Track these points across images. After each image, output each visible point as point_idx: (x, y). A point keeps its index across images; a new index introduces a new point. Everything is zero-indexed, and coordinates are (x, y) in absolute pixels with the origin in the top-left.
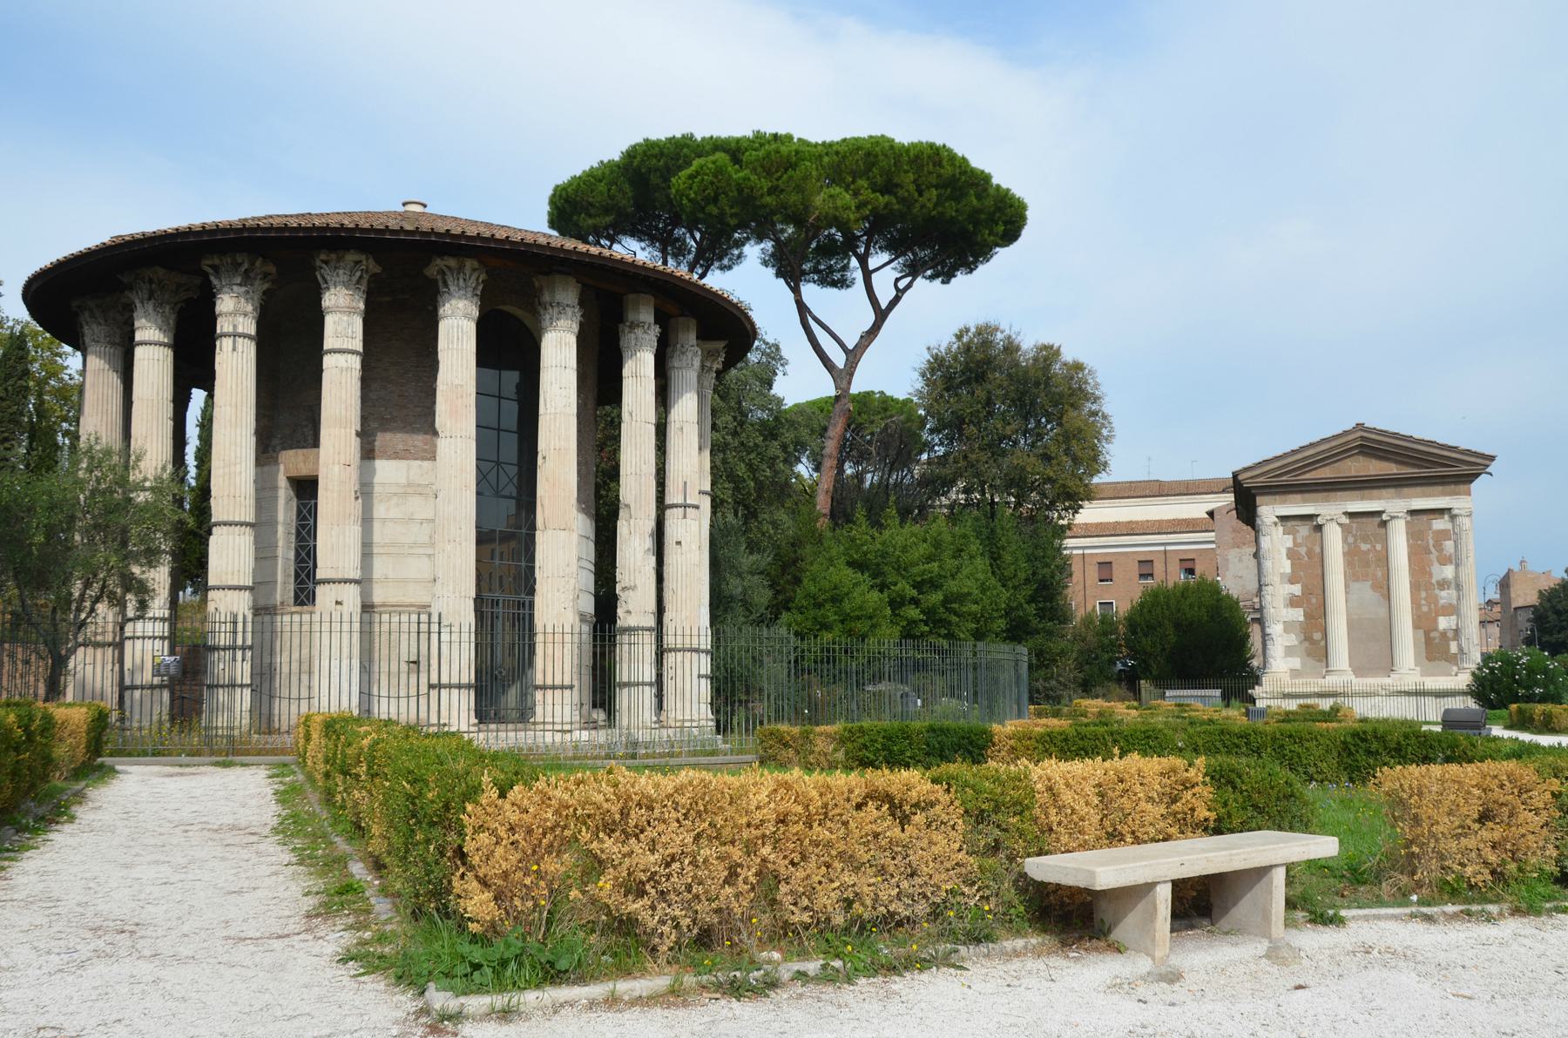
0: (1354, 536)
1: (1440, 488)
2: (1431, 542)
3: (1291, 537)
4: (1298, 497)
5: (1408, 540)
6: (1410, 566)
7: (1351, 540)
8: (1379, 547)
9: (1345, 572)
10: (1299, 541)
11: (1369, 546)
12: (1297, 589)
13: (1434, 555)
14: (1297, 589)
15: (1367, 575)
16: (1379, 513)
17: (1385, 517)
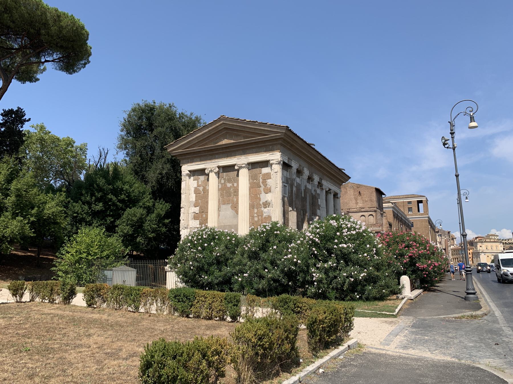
0: (224, 179)
2: (261, 180)
3: (196, 181)
5: (249, 180)
6: (250, 194)
7: (223, 181)
8: (235, 185)
9: (219, 199)
10: (200, 183)
11: (231, 184)
12: (197, 210)
13: (262, 189)
14: (197, 210)
15: (229, 200)
16: (234, 166)
17: (236, 168)
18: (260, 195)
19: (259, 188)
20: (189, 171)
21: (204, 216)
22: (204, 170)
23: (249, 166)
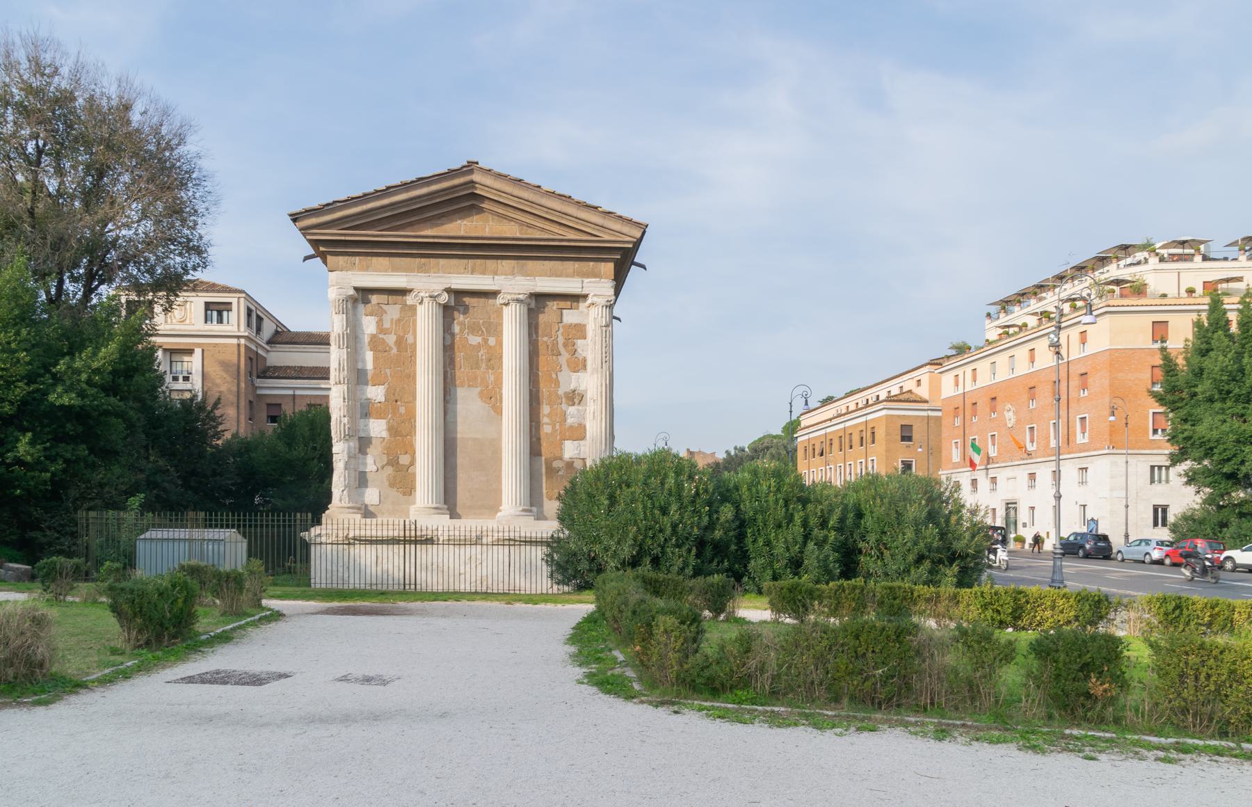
2: (561, 340)
11: (479, 339)
15: (476, 378)
19: (554, 357)
20: (356, 289)
21: (402, 410)
22: (403, 292)
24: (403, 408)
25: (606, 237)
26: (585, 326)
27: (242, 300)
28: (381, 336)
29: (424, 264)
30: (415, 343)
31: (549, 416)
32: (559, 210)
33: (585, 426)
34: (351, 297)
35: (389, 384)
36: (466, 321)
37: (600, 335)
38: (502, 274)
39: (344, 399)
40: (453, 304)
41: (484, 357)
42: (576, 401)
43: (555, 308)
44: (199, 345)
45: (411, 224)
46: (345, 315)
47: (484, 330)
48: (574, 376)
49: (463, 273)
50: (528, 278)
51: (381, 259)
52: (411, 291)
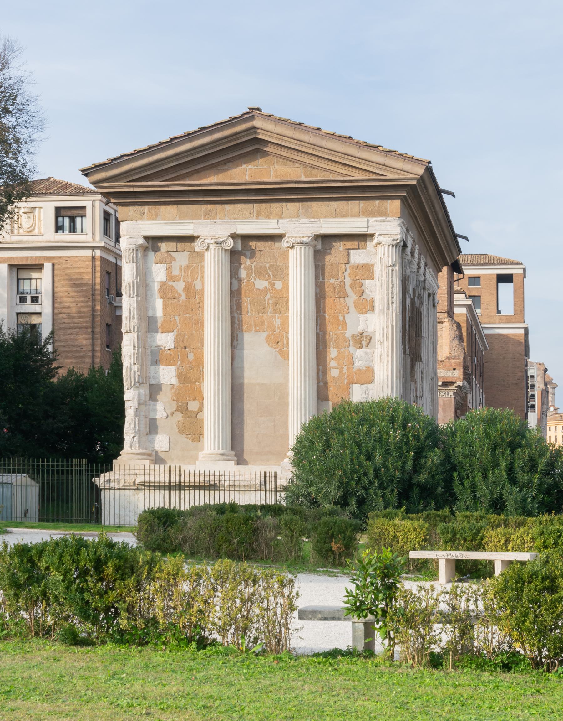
1: (363, 204)
2: (348, 281)
4: (171, 210)
8: (278, 285)
11: (265, 284)
15: (263, 322)
18: (346, 315)
19: (341, 299)
20: (146, 238)
21: (191, 356)
22: (191, 239)
23: (316, 243)
24: (192, 354)
25: (390, 176)
26: (372, 265)
27: (97, 203)
28: (170, 283)
29: (210, 211)
30: (203, 289)
31: (336, 359)
32: (340, 151)
33: (373, 369)
34: (141, 246)
35: (178, 331)
36: (253, 265)
37: (386, 275)
38: (287, 217)
39: (134, 347)
40: (240, 249)
41: (270, 302)
42: (364, 343)
43: (341, 249)
44: (48, 259)
45: (197, 171)
46: (135, 264)
47: (271, 273)
48: (362, 317)
49: (248, 218)
50: (313, 220)
51: (169, 208)
52: (198, 237)
